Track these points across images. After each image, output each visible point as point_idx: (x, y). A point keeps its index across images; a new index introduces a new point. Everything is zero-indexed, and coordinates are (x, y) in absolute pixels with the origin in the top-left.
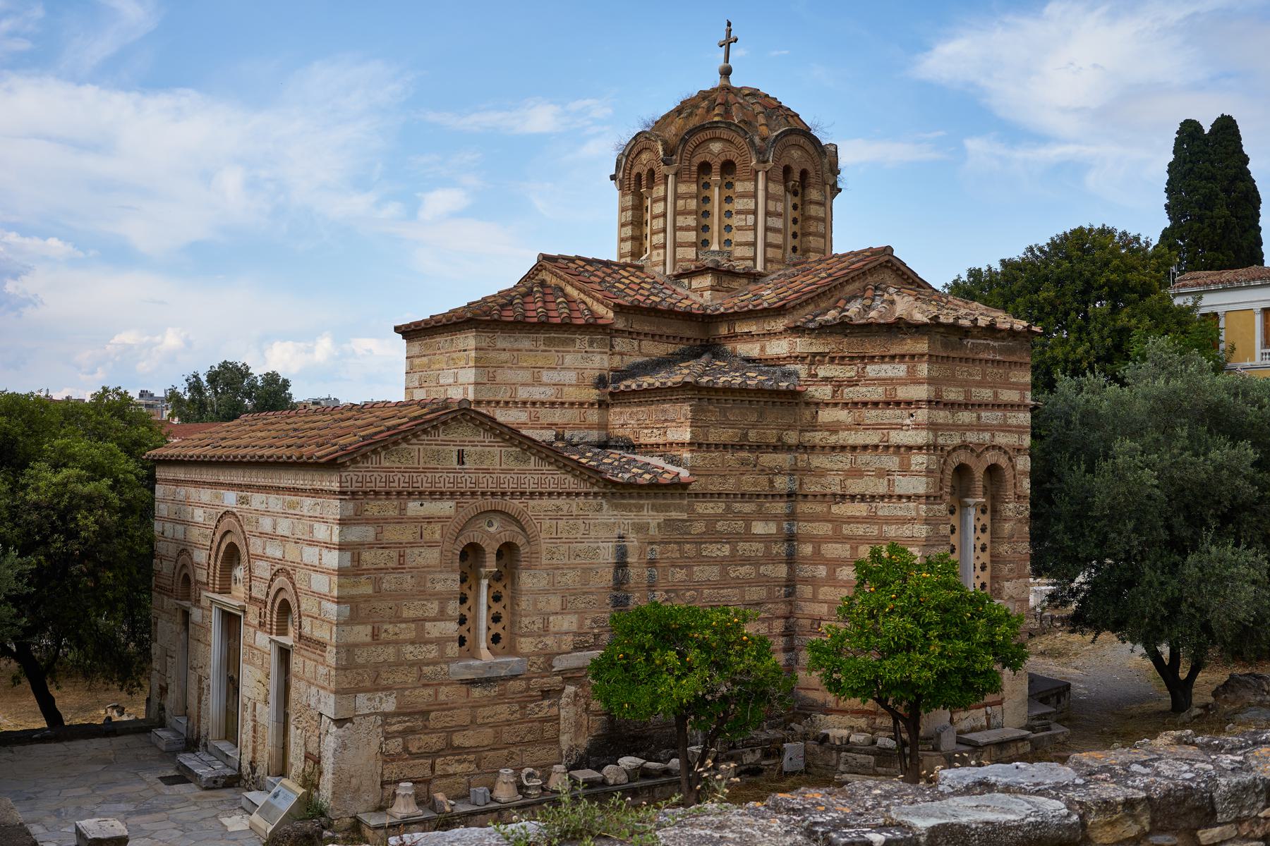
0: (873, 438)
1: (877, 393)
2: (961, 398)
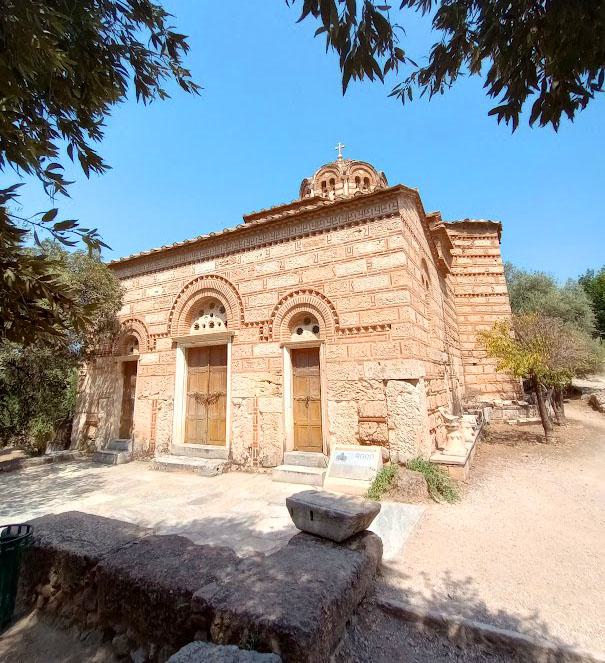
0: (482, 270)
1: (480, 252)
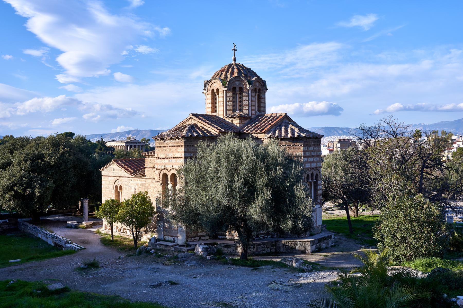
2: (164, 157)
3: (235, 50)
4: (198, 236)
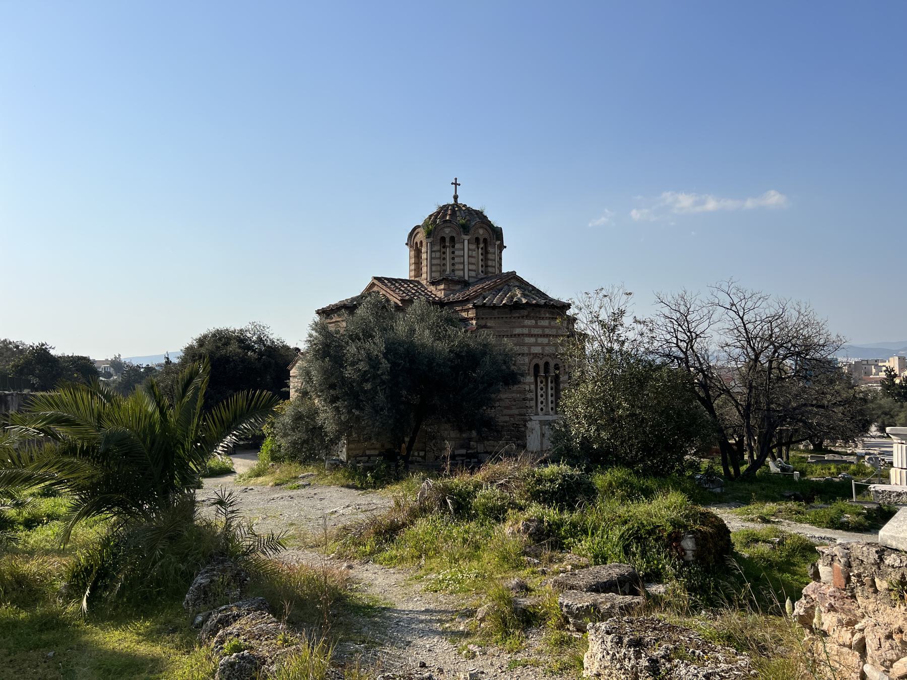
3: (456, 184)
4: (366, 456)
